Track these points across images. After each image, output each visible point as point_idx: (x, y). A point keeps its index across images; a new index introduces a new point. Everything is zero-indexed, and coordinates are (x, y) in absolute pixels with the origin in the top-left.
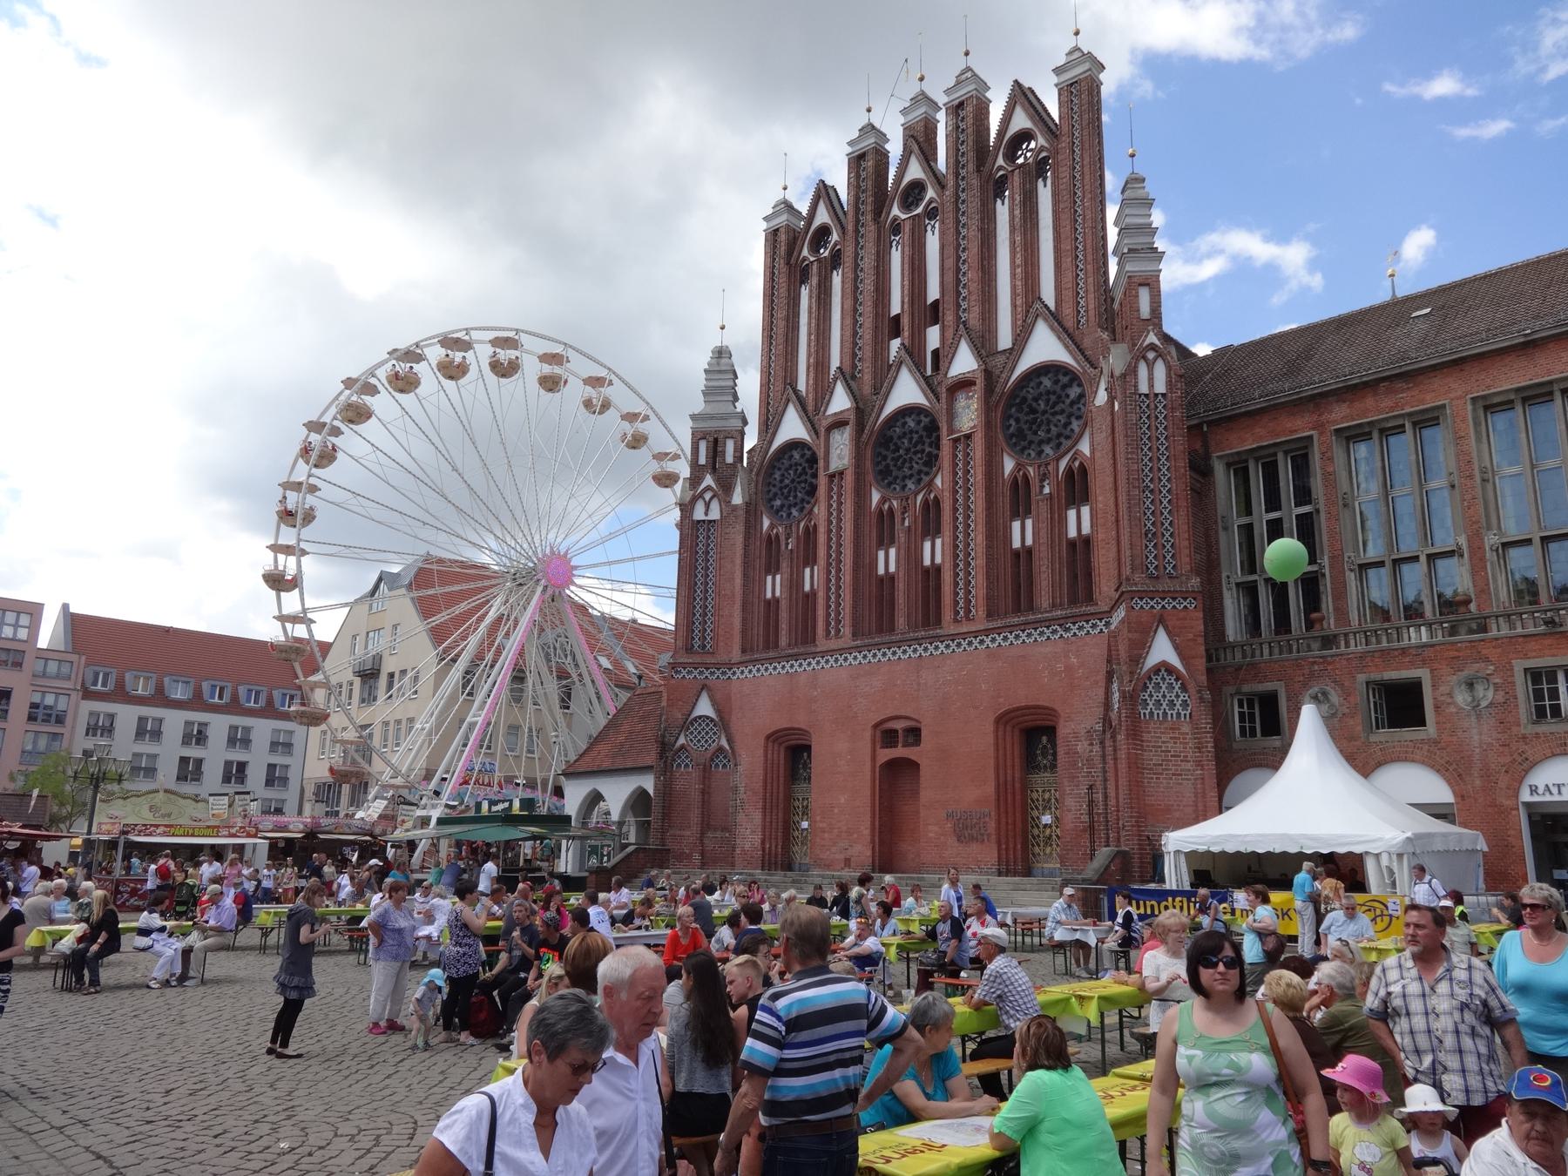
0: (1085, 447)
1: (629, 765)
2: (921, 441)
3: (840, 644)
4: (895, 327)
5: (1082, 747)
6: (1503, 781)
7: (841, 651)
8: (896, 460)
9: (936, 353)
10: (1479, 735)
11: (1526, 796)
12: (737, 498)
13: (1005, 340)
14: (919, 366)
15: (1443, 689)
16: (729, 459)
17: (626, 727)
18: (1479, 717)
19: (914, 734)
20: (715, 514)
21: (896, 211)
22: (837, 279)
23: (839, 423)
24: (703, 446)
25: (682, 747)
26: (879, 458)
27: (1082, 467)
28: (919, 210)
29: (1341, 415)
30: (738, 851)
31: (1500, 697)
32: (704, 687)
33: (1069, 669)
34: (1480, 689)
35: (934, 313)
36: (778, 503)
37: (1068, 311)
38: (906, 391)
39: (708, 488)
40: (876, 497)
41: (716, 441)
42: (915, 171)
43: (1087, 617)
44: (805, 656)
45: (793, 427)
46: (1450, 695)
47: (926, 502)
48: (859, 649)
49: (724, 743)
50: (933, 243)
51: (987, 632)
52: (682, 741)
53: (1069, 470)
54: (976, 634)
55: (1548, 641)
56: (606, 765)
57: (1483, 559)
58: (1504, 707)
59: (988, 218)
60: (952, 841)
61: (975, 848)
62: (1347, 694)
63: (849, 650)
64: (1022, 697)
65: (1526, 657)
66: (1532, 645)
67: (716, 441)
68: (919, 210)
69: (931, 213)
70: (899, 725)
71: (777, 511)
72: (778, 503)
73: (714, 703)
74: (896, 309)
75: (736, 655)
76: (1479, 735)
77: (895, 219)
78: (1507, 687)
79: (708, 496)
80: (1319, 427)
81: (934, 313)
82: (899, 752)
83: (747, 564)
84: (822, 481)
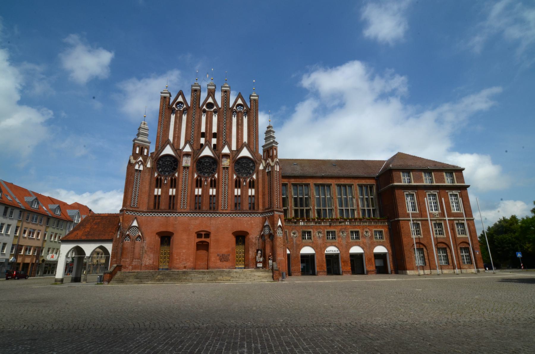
0: (254, 177)
1: (97, 239)
2: (210, 165)
3: (185, 211)
4: (203, 135)
5: (254, 241)
6: (323, 249)
7: (185, 213)
8: (203, 167)
9: (214, 145)
10: (320, 241)
11: (326, 252)
12: (149, 165)
13: (234, 148)
14: (210, 148)
16: (145, 154)
17: (88, 226)
19: (208, 235)
20: (141, 168)
21: (204, 107)
22: (184, 117)
23: (187, 155)
24: (138, 149)
25: (128, 235)
26: (197, 166)
27: (253, 181)
28: (212, 110)
29: (293, 181)
30: (143, 265)
32: (136, 218)
33: (251, 223)
35: (215, 135)
36: (160, 169)
37: (251, 147)
38: (207, 152)
39: (141, 161)
40: (196, 176)
41: (142, 148)
42: (210, 100)
43: (256, 213)
44: (172, 213)
45: (168, 150)
47: (211, 180)
48: (192, 213)
49: (140, 234)
50: (215, 119)
51: (231, 213)
52: (128, 233)
53: (250, 181)
54: (227, 213)
56: (84, 238)
58: (324, 237)
59: (231, 119)
60: (219, 261)
61: (225, 263)
62: (299, 233)
63: (189, 213)
64: (240, 228)
67: (142, 148)
68: (212, 110)
69: (215, 112)
70: (203, 233)
71: (161, 172)
72: (160, 169)
73: (138, 223)
74: (203, 130)
75: (145, 209)
76: (320, 241)
77: (204, 109)
79: (140, 163)
80: (289, 182)
81: (215, 135)
82: (203, 239)
83: (150, 184)
84: (182, 169)
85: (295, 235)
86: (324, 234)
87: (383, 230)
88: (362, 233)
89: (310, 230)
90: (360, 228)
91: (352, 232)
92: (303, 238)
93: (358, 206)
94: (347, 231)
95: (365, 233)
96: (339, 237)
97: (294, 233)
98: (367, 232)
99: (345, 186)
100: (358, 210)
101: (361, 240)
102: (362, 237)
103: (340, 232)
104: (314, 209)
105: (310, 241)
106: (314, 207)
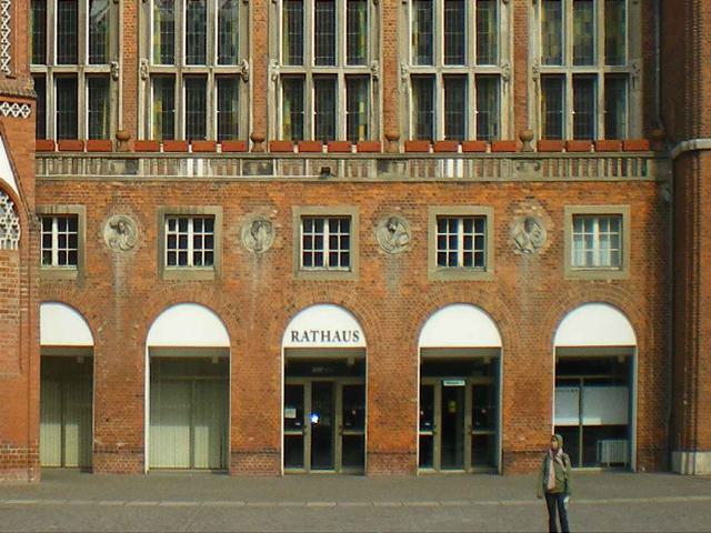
15: (232, 229)
18: (260, 260)
31: (279, 243)
34: (263, 233)
46: (238, 236)
55: (323, 190)
57: (265, 89)
58: (279, 252)
62: (146, 227)
65: (303, 204)
66: (310, 193)
78: (285, 233)
85: (123, 239)
86: (285, 233)
87: (625, 210)
88: (504, 230)
89: (208, 210)
90: (490, 200)
91: (446, 222)
92: (171, 261)
93: (521, 54)
94: (414, 220)
95: (517, 229)
96: (369, 251)
97: (117, 228)
98: (528, 223)
99: (77, 158)
100: (521, 84)
101: (488, 273)
102: (500, 251)
103: (374, 220)
104: (262, 76)
105: (206, 272)
106: (262, 62)
